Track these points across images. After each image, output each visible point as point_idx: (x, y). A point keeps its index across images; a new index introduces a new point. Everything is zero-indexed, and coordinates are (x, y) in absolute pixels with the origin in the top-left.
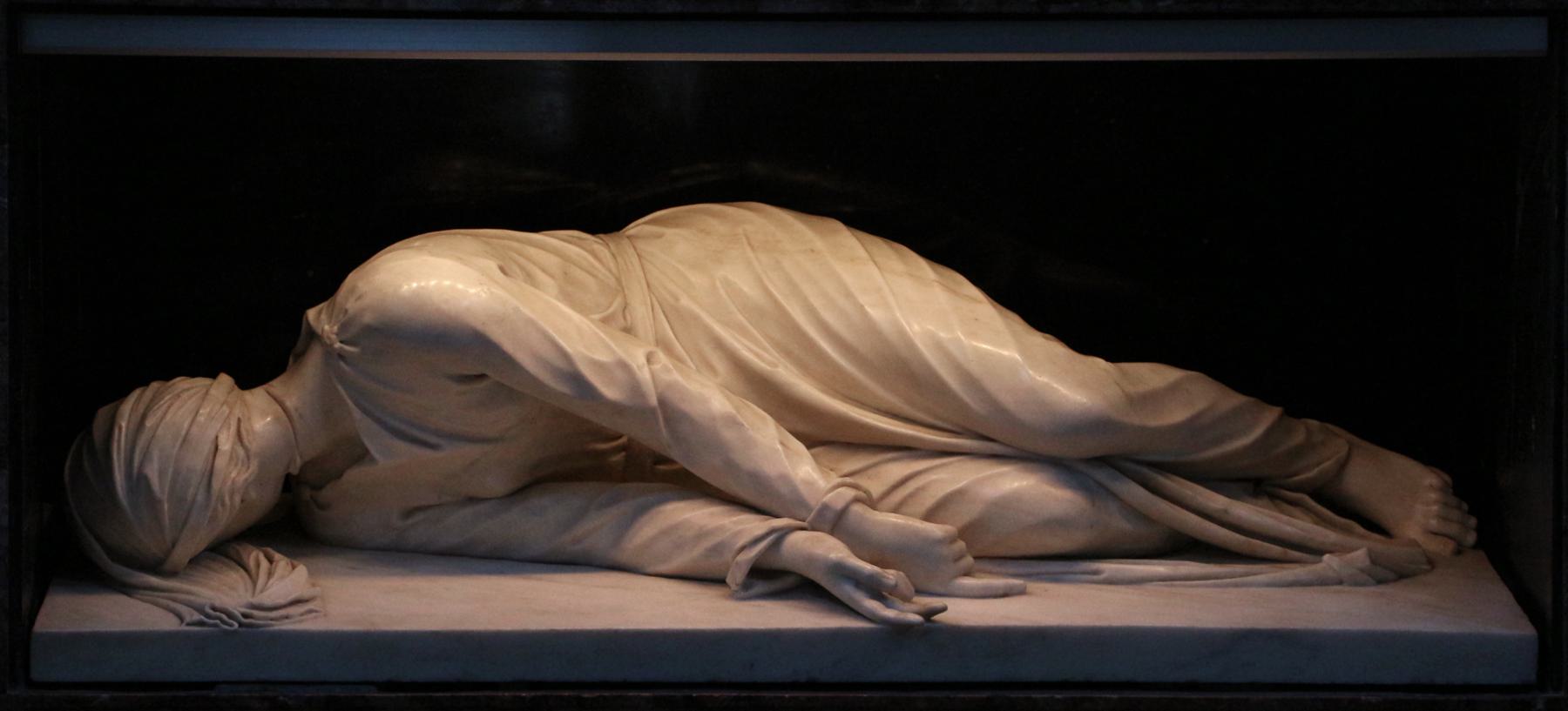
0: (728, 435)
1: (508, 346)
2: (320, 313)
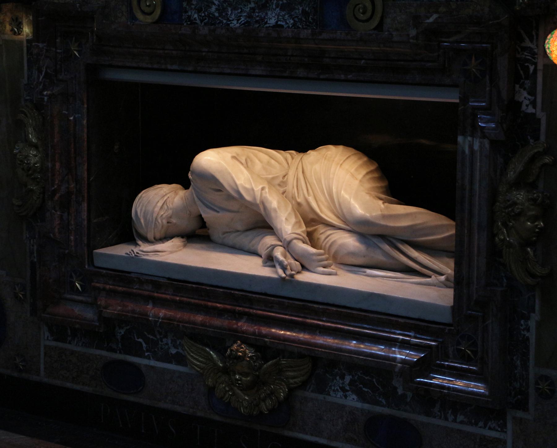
0: (273, 214)
1: (221, 180)
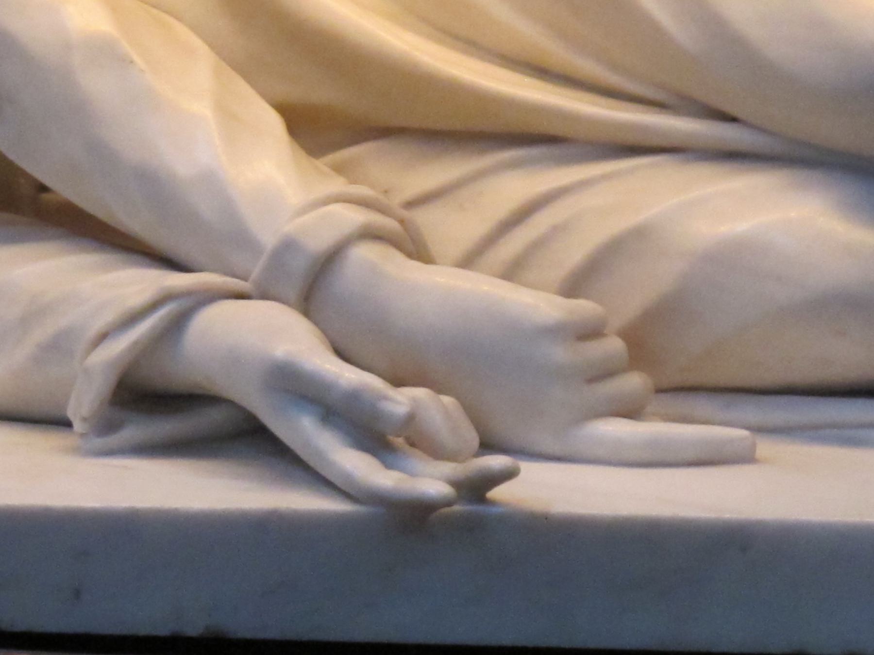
0: (98, 85)
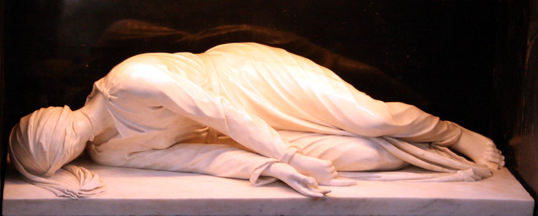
2: (101, 83)
